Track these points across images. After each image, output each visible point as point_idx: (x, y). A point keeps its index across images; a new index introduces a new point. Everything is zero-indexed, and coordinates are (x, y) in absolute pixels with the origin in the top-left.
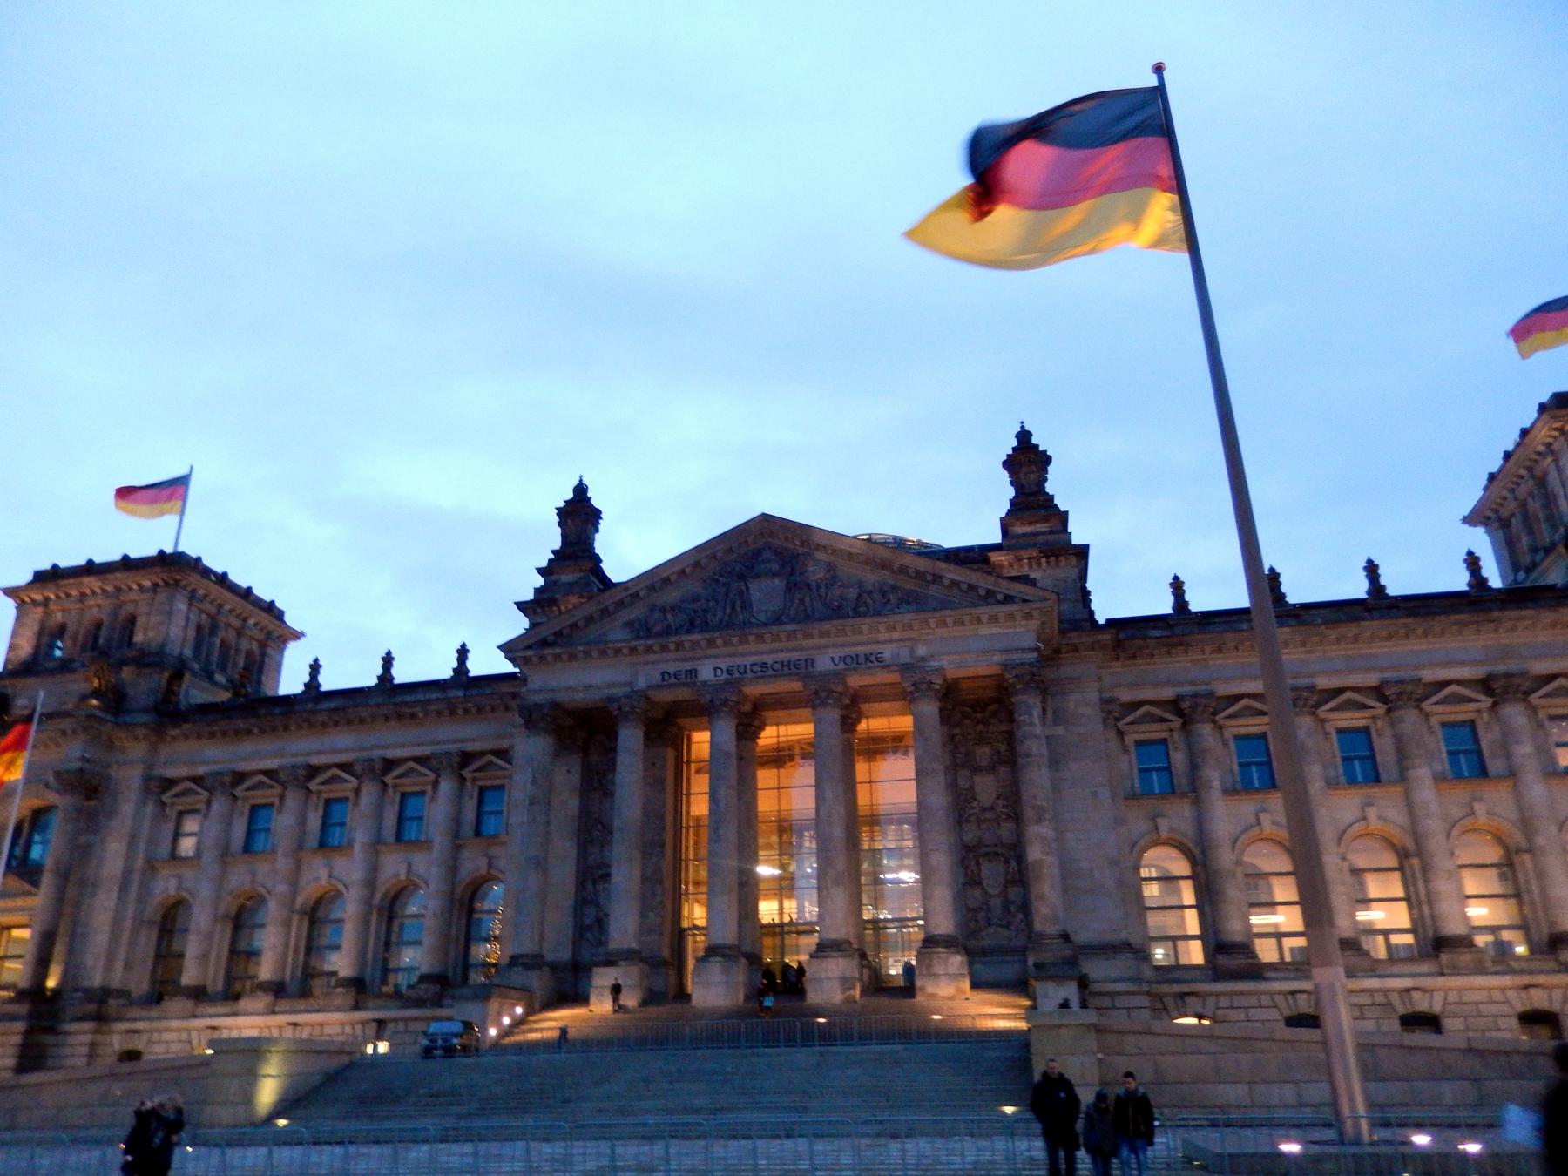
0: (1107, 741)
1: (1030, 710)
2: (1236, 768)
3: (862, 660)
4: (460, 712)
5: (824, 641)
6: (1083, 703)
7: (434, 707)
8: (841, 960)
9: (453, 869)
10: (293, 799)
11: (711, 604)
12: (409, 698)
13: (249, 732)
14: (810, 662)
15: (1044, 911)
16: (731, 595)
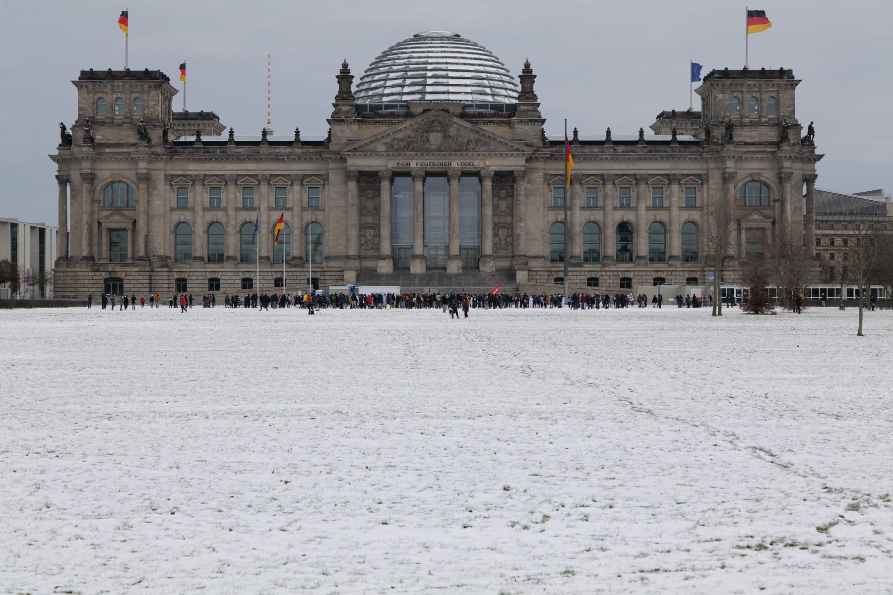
0: (544, 188)
1: (522, 186)
2: (586, 199)
3: (467, 164)
4: (303, 159)
5: (455, 157)
6: (538, 177)
7: (291, 157)
8: (458, 261)
9: (302, 219)
10: (232, 188)
11: (416, 139)
12: (277, 150)
13: (211, 159)
14: (450, 164)
15: (520, 248)
16: (423, 138)
